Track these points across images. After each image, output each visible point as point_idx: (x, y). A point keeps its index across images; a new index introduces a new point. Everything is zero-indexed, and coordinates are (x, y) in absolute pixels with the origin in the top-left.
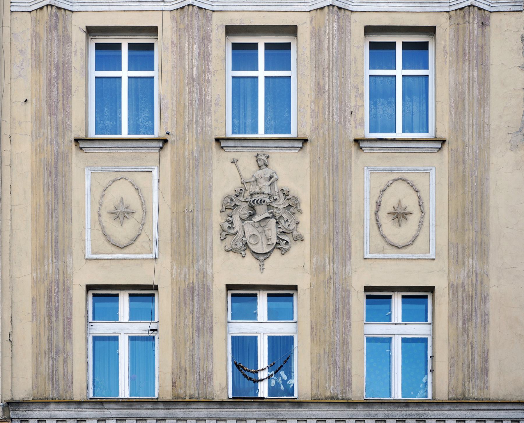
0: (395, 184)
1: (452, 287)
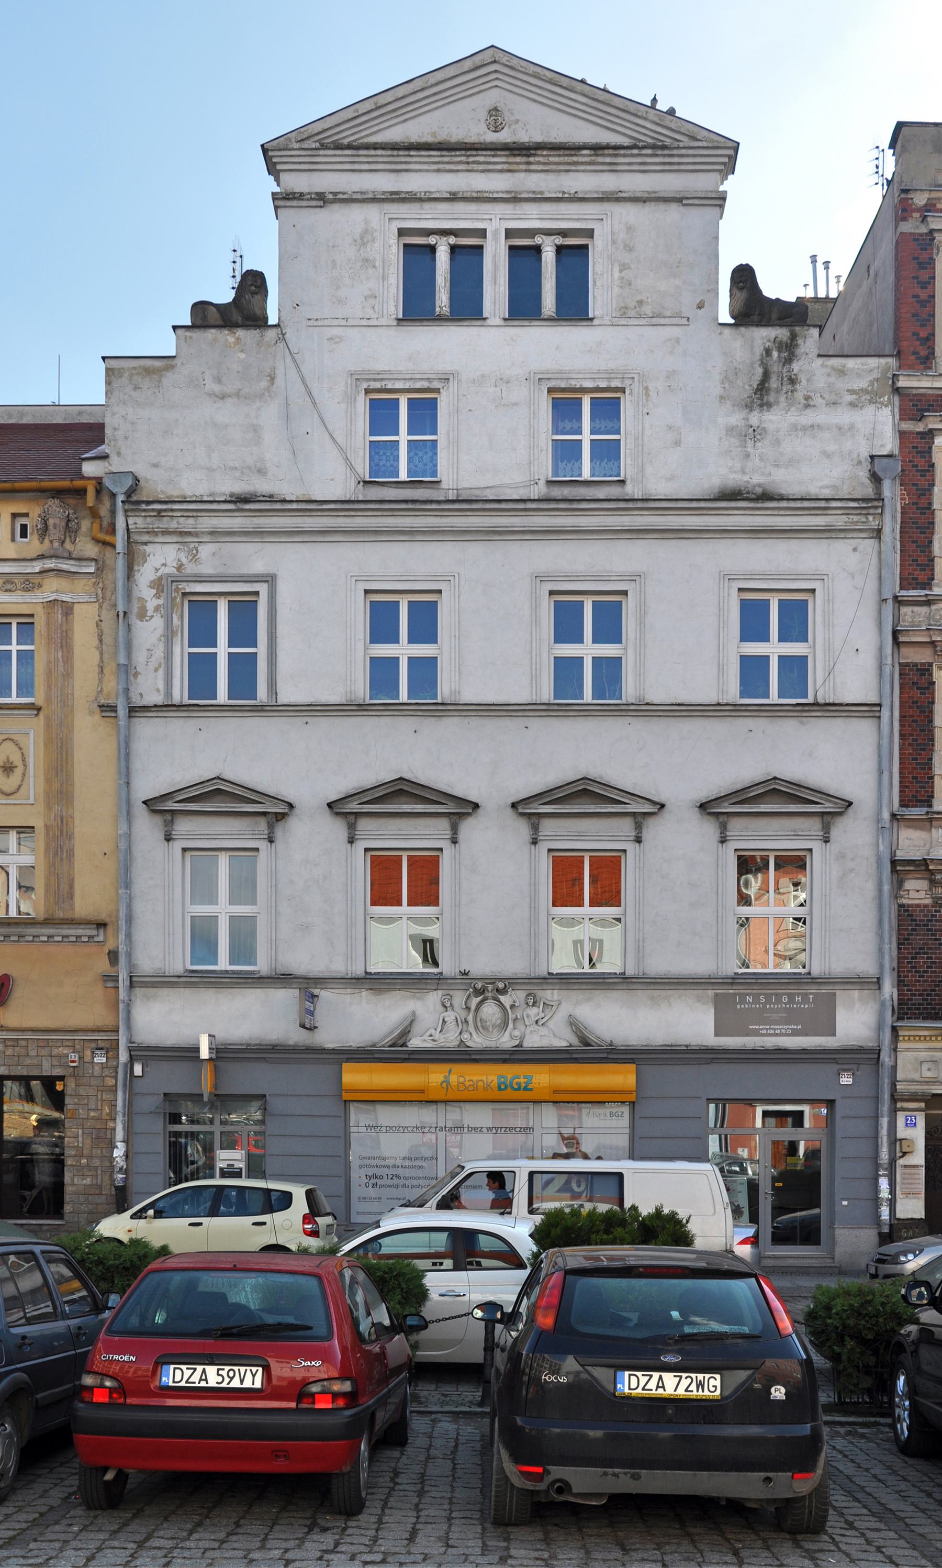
0: (5, 743)
1: (46, 826)
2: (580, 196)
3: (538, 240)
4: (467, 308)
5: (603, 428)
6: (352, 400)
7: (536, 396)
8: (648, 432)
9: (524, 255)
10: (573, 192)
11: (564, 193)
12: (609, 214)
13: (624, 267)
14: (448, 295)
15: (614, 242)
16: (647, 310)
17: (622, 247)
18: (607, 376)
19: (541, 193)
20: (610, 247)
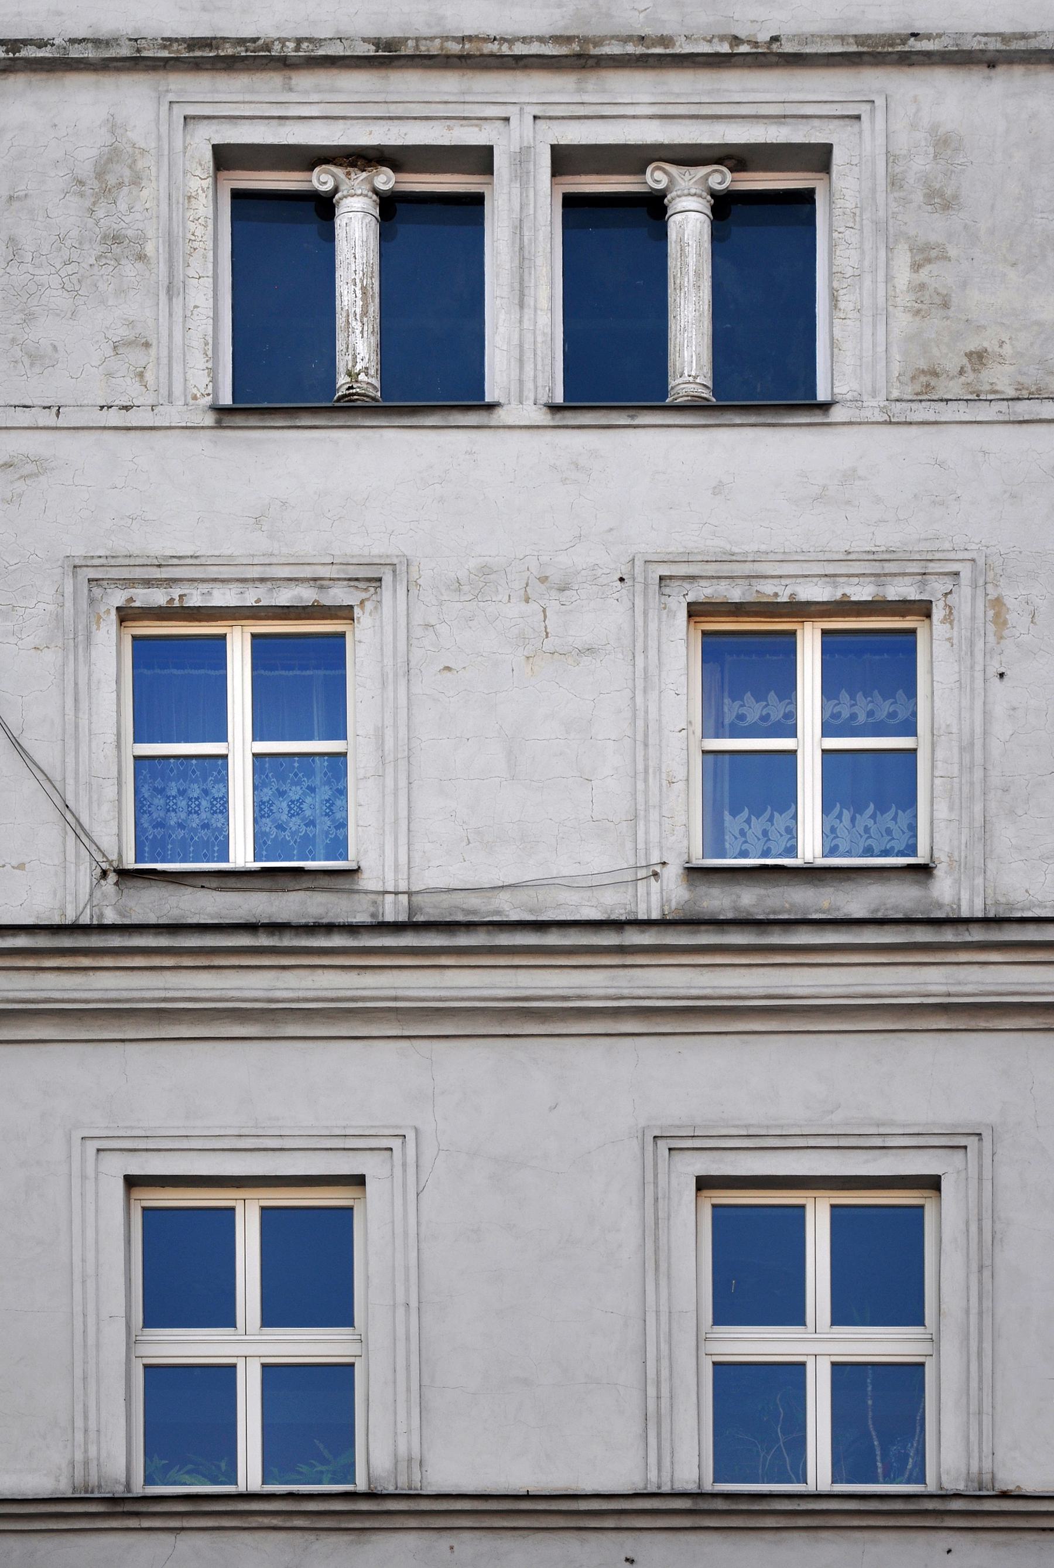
2: (788, 48)
3: (656, 178)
4: (435, 371)
5: (862, 718)
6: (79, 642)
7: (653, 626)
8: (1001, 729)
9: (610, 227)
10: (764, 37)
11: (736, 40)
12: (880, 102)
13: (925, 255)
14: (375, 340)
15: (894, 182)
16: (1000, 377)
17: (918, 197)
18: (876, 568)
19: (665, 40)
20: (881, 198)
